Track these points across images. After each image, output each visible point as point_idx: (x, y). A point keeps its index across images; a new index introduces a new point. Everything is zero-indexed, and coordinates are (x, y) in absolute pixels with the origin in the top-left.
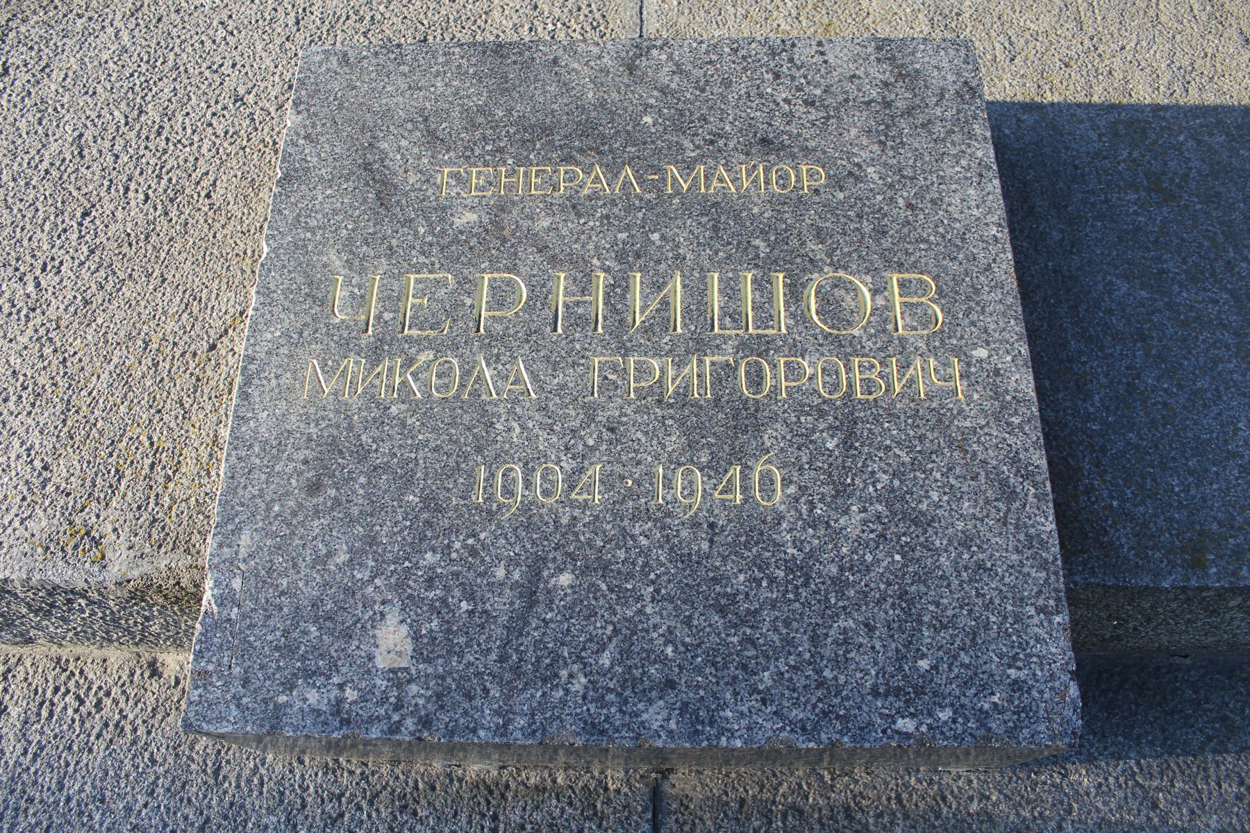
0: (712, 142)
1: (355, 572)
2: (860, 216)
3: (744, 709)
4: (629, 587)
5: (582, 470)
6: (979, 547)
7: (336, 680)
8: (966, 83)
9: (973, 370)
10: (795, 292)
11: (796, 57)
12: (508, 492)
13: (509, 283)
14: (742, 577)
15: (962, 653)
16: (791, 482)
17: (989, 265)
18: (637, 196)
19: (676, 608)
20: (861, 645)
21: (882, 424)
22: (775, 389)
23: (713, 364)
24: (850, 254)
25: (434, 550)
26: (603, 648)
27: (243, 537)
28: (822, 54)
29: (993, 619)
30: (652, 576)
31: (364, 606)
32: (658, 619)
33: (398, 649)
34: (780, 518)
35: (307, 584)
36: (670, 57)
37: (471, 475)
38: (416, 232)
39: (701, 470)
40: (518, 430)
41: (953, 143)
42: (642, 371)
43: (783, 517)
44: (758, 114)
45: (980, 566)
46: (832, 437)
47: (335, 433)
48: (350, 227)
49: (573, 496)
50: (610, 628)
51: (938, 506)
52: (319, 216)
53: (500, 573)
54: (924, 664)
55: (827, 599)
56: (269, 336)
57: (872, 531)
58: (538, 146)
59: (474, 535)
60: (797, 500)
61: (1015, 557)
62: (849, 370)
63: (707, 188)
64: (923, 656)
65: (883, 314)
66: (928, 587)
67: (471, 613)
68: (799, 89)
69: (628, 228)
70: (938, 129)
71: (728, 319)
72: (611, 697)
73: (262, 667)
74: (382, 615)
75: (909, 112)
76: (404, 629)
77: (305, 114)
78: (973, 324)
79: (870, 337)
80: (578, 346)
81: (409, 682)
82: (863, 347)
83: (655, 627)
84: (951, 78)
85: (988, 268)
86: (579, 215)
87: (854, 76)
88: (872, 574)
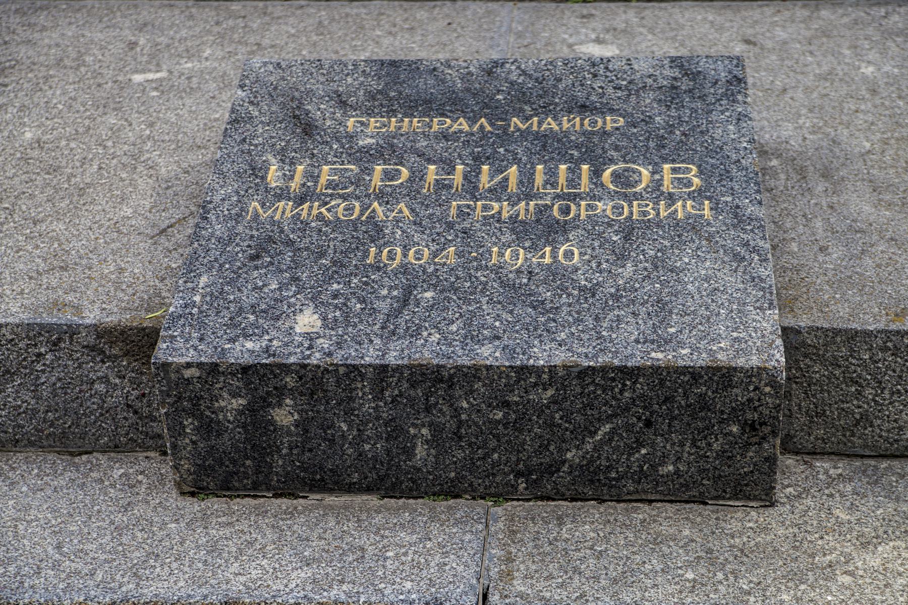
0: (544, 107)
2: (648, 139)
3: (547, 348)
7: (267, 337)
10: (597, 173)
11: (610, 67)
13: (397, 170)
19: (503, 306)
25: (339, 283)
26: (453, 322)
28: (630, 65)
36: (519, 68)
38: (331, 148)
40: (400, 233)
42: (485, 208)
47: (271, 234)
50: (457, 315)
54: (672, 330)
55: (606, 302)
56: (223, 192)
63: (539, 127)
72: (455, 343)
73: (213, 333)
74: (301, 310)
76: (316, 316)
81: (319, 337)
86: (447, 140)
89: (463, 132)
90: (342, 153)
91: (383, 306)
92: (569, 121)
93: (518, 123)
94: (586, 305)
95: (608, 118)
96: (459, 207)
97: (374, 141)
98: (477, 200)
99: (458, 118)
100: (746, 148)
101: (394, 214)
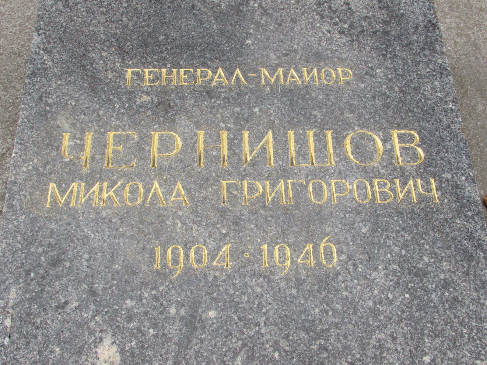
0: (286, 55)
1: (83, 313)
4: (251, 317)
5: (219, 248)
6: (454, 288)
8: (430, 21)
9: (443, 185)
10: (339, 141)
12: (176, 261)
14: (317, 310)
15: (448, 352)
16: (342, 252)
17: (449, 125)
18: (244, 86)
20: (389, 349)
21: (393, 218)
22: (330, 198)
23: (293, 184)
24: (369, 119)
27: (11, 293)
29: (465, 331)
30: (264, 310)
31: (89, 334)
32: (269, 337)
33: (111, 360)
34: (338, 274)
35: (53, 321)
37: (152, 252)
38: (114, 107)
39: (289, 246)
40: (180, 225)
41: (425, 55)
42: (252, 189)
43: (339, 274)
44: (313, 39)
45: (455, 299)
46: (365, 226)
48: (73, 104)
49: (215, 263)
50: (240, 343)
51: (428, 265)
52: (54, 97)
53: (173, 311)
56: (25, 169)
57: (391, 281)
58: (185, 56)
59: (156, 288)
60: (346, 263)
61: (474, 294)
62: (372, 186)
63: (285, 80)
64: (426, 354)
65: (389, 152)
66: (426, 313)
67: (156, 336)
68: (336, 24)
69: (240, 105)
70: (416, 48)
71: (301, 158)
74: (101, 340)
75: (399, 37)
76: (115, 348)
77: (43, 36)
78: (442, 159)
79: (384, 167)
80: (214, 175)
82: (380, 173)
83: (267, 341)
84: (421, 18)
85: (449, 127)
86: (211, 98)
87: (366, 17)
88: (393, 306)
89: (222, 87)
90: (123, 114)
91: (174, 330)
92: (309, 73)
93: (267, 74)
94: (350, 326)
95: (340, 70)
96: (229, 186)
97: (149, 98)
98: (243, 178)
99: (217, 68)
100: (452, 110)
101: (172, 199)
